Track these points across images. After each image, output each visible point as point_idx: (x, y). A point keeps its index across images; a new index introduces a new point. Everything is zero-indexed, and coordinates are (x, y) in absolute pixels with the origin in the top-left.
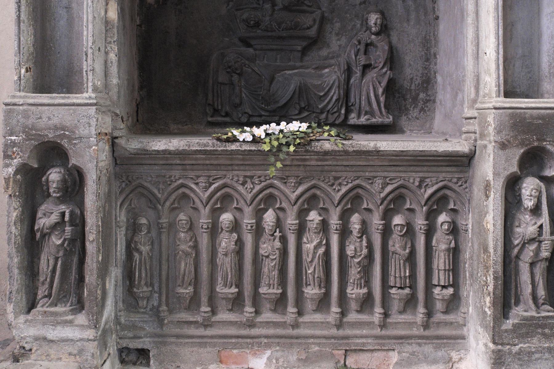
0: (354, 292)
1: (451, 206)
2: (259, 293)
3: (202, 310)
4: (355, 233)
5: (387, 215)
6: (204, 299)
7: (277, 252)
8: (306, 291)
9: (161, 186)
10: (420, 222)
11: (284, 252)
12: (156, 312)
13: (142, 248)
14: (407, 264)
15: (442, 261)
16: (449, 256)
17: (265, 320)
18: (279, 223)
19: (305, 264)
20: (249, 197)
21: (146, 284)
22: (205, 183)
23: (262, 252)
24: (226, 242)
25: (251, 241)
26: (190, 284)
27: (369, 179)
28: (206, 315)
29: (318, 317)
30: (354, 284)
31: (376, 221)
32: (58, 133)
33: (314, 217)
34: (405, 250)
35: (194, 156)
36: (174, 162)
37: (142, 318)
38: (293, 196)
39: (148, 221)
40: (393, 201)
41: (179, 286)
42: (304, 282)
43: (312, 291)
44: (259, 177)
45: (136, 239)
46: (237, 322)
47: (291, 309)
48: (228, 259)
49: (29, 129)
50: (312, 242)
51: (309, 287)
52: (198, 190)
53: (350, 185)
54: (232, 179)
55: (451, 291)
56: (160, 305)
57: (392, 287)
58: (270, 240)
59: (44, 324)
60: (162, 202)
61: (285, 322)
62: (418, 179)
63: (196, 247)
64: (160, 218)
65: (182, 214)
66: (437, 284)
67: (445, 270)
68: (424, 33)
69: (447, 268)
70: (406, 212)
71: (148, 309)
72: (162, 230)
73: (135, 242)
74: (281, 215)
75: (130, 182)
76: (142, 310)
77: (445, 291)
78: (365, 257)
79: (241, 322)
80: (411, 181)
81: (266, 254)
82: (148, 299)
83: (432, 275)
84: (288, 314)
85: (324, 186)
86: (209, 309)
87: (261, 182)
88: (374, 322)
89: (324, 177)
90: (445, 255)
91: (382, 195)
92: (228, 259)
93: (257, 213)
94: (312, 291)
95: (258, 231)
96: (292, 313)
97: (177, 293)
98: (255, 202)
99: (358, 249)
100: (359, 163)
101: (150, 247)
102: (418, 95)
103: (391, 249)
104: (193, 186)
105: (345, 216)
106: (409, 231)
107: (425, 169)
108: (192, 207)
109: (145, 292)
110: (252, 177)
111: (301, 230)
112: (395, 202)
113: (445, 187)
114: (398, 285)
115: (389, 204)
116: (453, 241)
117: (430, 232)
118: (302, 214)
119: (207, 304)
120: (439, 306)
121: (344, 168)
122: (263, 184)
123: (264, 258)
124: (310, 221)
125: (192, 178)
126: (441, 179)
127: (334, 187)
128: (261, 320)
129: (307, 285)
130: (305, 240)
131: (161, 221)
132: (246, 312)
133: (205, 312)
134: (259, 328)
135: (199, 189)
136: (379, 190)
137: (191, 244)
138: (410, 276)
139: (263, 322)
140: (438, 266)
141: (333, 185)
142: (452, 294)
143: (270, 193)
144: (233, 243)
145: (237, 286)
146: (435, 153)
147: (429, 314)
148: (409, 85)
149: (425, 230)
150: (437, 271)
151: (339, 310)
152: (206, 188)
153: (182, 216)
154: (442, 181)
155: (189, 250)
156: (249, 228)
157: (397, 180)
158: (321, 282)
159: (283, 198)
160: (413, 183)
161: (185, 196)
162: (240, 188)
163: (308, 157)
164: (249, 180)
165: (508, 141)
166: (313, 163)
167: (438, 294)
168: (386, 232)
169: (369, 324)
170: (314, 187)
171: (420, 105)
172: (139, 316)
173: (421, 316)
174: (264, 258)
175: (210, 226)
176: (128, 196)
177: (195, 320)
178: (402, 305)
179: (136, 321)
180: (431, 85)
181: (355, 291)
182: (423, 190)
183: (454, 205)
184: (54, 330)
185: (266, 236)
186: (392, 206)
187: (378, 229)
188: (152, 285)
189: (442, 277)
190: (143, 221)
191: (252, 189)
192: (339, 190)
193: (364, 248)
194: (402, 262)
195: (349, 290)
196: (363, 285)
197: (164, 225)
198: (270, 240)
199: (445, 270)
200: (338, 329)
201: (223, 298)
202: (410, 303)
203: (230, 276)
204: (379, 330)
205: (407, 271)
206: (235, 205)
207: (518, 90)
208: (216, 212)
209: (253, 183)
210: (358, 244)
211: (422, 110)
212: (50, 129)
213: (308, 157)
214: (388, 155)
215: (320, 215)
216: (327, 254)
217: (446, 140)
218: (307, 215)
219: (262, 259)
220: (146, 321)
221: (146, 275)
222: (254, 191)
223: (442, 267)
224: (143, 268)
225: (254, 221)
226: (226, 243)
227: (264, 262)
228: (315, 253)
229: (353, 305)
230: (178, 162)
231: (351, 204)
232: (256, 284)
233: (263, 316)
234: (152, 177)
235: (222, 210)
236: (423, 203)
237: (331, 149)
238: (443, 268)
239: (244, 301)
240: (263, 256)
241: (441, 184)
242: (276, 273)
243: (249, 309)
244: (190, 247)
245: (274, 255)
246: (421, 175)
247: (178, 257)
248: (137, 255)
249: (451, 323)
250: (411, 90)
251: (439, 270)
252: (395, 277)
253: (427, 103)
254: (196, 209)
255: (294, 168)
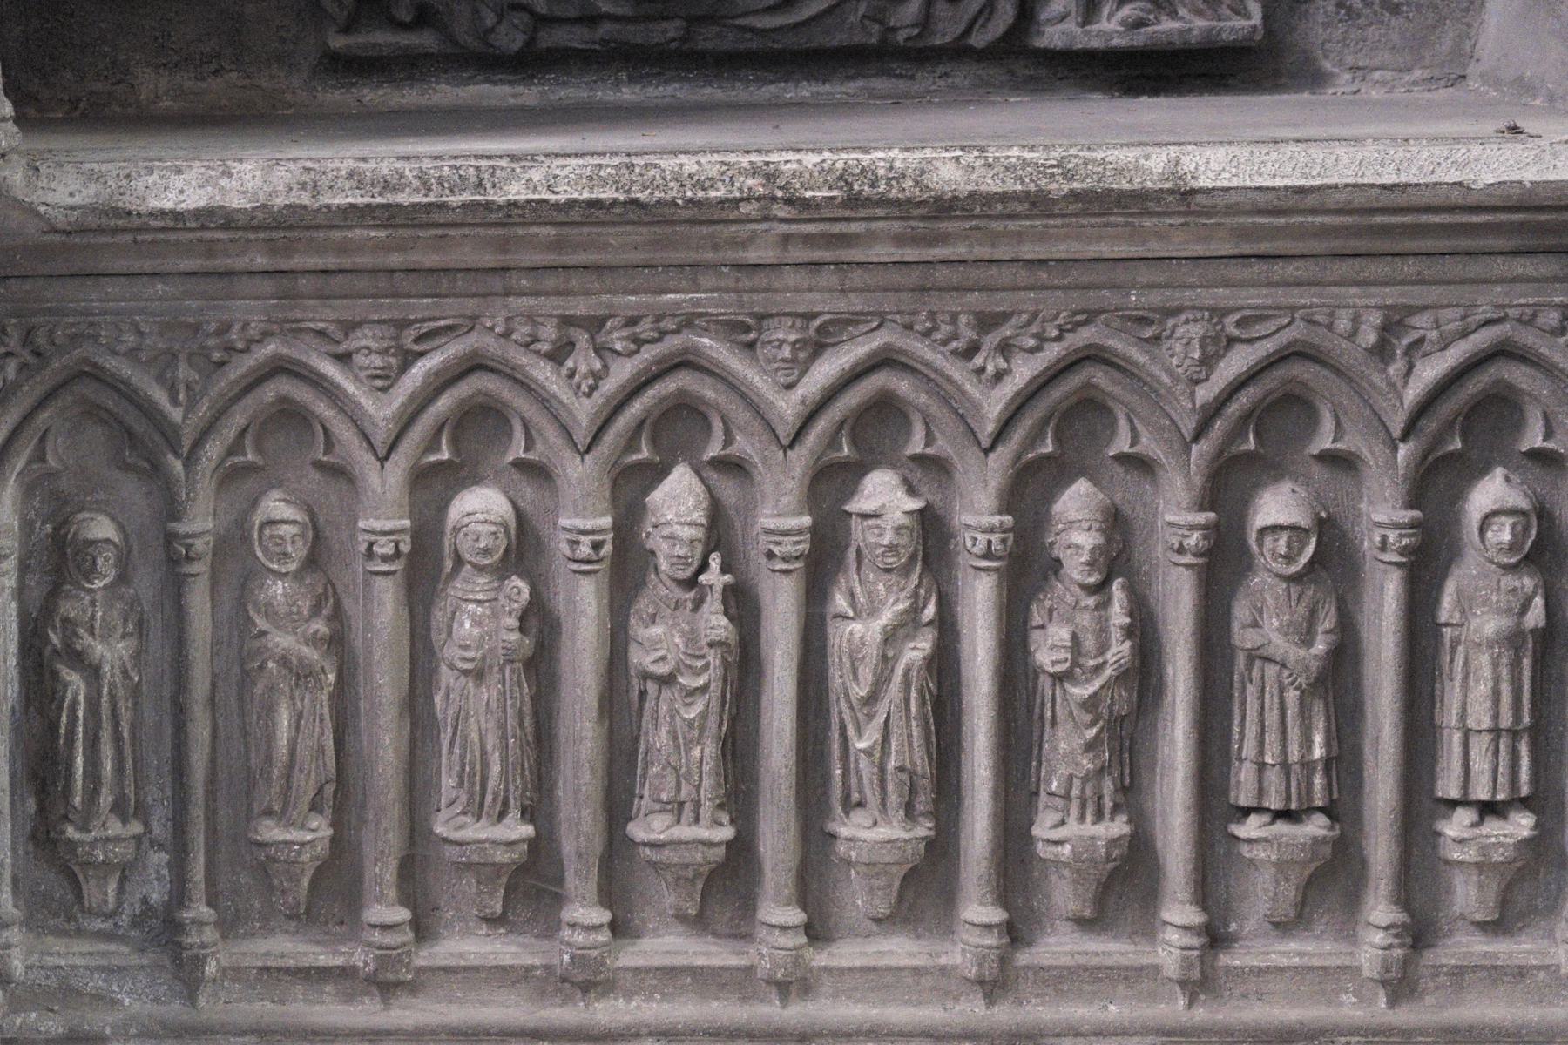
0: (1068, 833)
1: (1534, 438)
2: (633, 843)
3: (374, 919)
4: (1076, 568)
5: (1226, 488)
6: (382, 871)
7: (714, 658)
8: (844, 831)
9: (183, 372)
10: (1382, 514)
11: (745, 663)
12: (164, 930)
13: (98, 649)
14: (1318, 707)
15: (1482, 689)
16: (1515, 665)
17: (657, 961)
18: (719, 532)
19: (840, 710)
20: (584, 412)
21: (119, 808)
22: (384, 352)
23: (640, 658)
24: (477, 618)
25: (592, 610)
26: (315, 807)
27: (1143, 321)
28: (389, 939)
29: (899, 950)
30: (1067, 797)
31: (1175, 514)
33: (884, 497)
34: (1307, 642)
35: (337, 235)
36: (241, 263)
37: (104, 954)
38: (787, 407)
39: (121, 528)
40: (1259, 418)
41: (269, 813)
42: (837, 791)
43: (872, 833)
44: (632, 322)
45: (67, 608)
46: (529, 969)
47: (779, 912)
48: (489, 693)
50: (873, 612)
51: (858, 816)
52: (350, 387)
53: (1053, 352)
54: (506, 335)
55: (1522, 824)
56: (180, 894)
57: (1246, 812)
58: (678, 605)
60: (187, 443)
61: (749, 970)
62: (1376, 318)
63: (338, 643)
64: (176, 517)
65: (276, 494)
66: (1454, 793)
67: (1495, 731)
69: (1506, 721)
70: (1317, 470)
71: (124, 920)
72: (188, 569)
73: (66, 620)
74: (729, 490)
75: (37, 354)
76: (98, 924)
77: (1494, 829)
78: (1121, 677)
79: (548, 968)
80: (1343, 324)
81: (662, 669)
82: (126, 872)
83: (1434, 759)
84: (762, 932)
85: (929, 355)
86: (402, 914)
87: (639, 342)
88: (1156, 969)
89: (932, 315)
90: (1495, 665)
91: (1205, 394)
92: (489, 693)
93: (615, 484)
94: (872, 833)
95: (627, 565)
96: (784, 928)
97: (261, 845)
98: (609, 437)
99: (1089, 643)
100: (1092, 250)
101: (132, 643)
103: (1243, 638)
104: (330, 369)
105: (1028, 494)
106: (1331, 558)
107: (1410, 268)
108: (318, 465)
109: (117, 839)
110: (595, 324)
111: (823, 560)
112: (1266, 425)
113: (1501, 352)
114: (1274, 802)
115: (1237, 432)
116: (1538, 601)
117: (1427, 562)
118: (831, 484)
119: (392, 893)
120: (1468, 895)
121: (1023, 276)
122: (648, 353)
123: (651, 687)
124: (865, 516)
125: (321, 333)
126: (1485, 311)
127: (978, 361)
128: (640, 962)
129: (849, 805)
130: (840, 602)
131: (182, 528)
132: (573, 926)
133: (385, 927)
134: (629, 996)
135: (356, 378)
136: (1188, 369)
137: (320, 626)
138: (1328, 762)
139: (647, 970)
140: (1463, 716)
141: (971, 351)
142: (1526, 842)
143: (681, 392)
144: (513, 622)
145: (528, 814)
146: (1456, 197)
147: (1418, 933)
149: (1403, 551)
150: (1457, 737)
151: (996, 915)
152: (385, 380)
153: (276, 506)
154: (1488, 322)
155: (312, 654)
156: (585, 550)
157: (1271, 326)
158: (913, 791)
159: (740, 415)
160: (1352, 335)
161: (291, 416)
162: (543, 373)
163: (854, 227)
164: (582, 338)
166: (882, 252)
167: (1462, 841)
168: (1223, 563)
169: (1136, 977)
170: (884, 360)
172: (86, 946)
173: (1379, 938)
174: (651, 687)
175: (405, 548)
176: (27, 418)
177: (339, 961)
178: (1290, 892)
179: (74, 967)
181: (1073, 828)
182: (1396, 368)
183: (1548, 435)
185: (660, 589)
186: (1251, 444)
187: (1181, 550)
188: (142, 812)
189: (1481, 764)
190: (102, 528)
191: (597, 377)
192: (999, 376)
193: (1116, 634)
194: (1292, 695)
195: (1043, 828)
196: (1108, 804)
197: (199, 545)
198: (678, 605)
199: (1495, 731)
200: (990, 1000)
201: (469, 866)
202: (1330, 882)
203: (495, 769)
204: (1182, 1002)
205: (1318, 739)
206: (517, 450)
208: (433, 485)
209: (599, 351)
210: (1085, 620)
213: (854, 227)
214: (1233, 210)
215: (912, 491)
216: (945, 664)
217: (1514, 130)
218: (851, 491)
219: (643, 694)
220: (120, 969)
221: (119, 769)
222: (609, 386)
223: (1480, 717)
224: (106, 735)
225: (606, 521)
226: (477, 623)
227: (649, 705)
228: (886, 661)
229: (1065, 896)
230: (261, 262)
231: (1058, 439)
232: (617, 807)
233: (646, 943)
234: (141, 334)
235: (459, 475)
236: (1397, 428)
237: (964, 189)
238: (1486, 723)
239: (560, 880)
240: (646, 676)
241: (1482, 339)
242: (706, 751)
243: (585, 912)
244: (314, 641)
245: (697, 673)
246: (1391, 295)
247: (258, 690)
248: (74, 681)
249: (1521, 972)
251: (1467, 734)
252: (1261, 766)
254: (339, 473)
255: (791, 278)
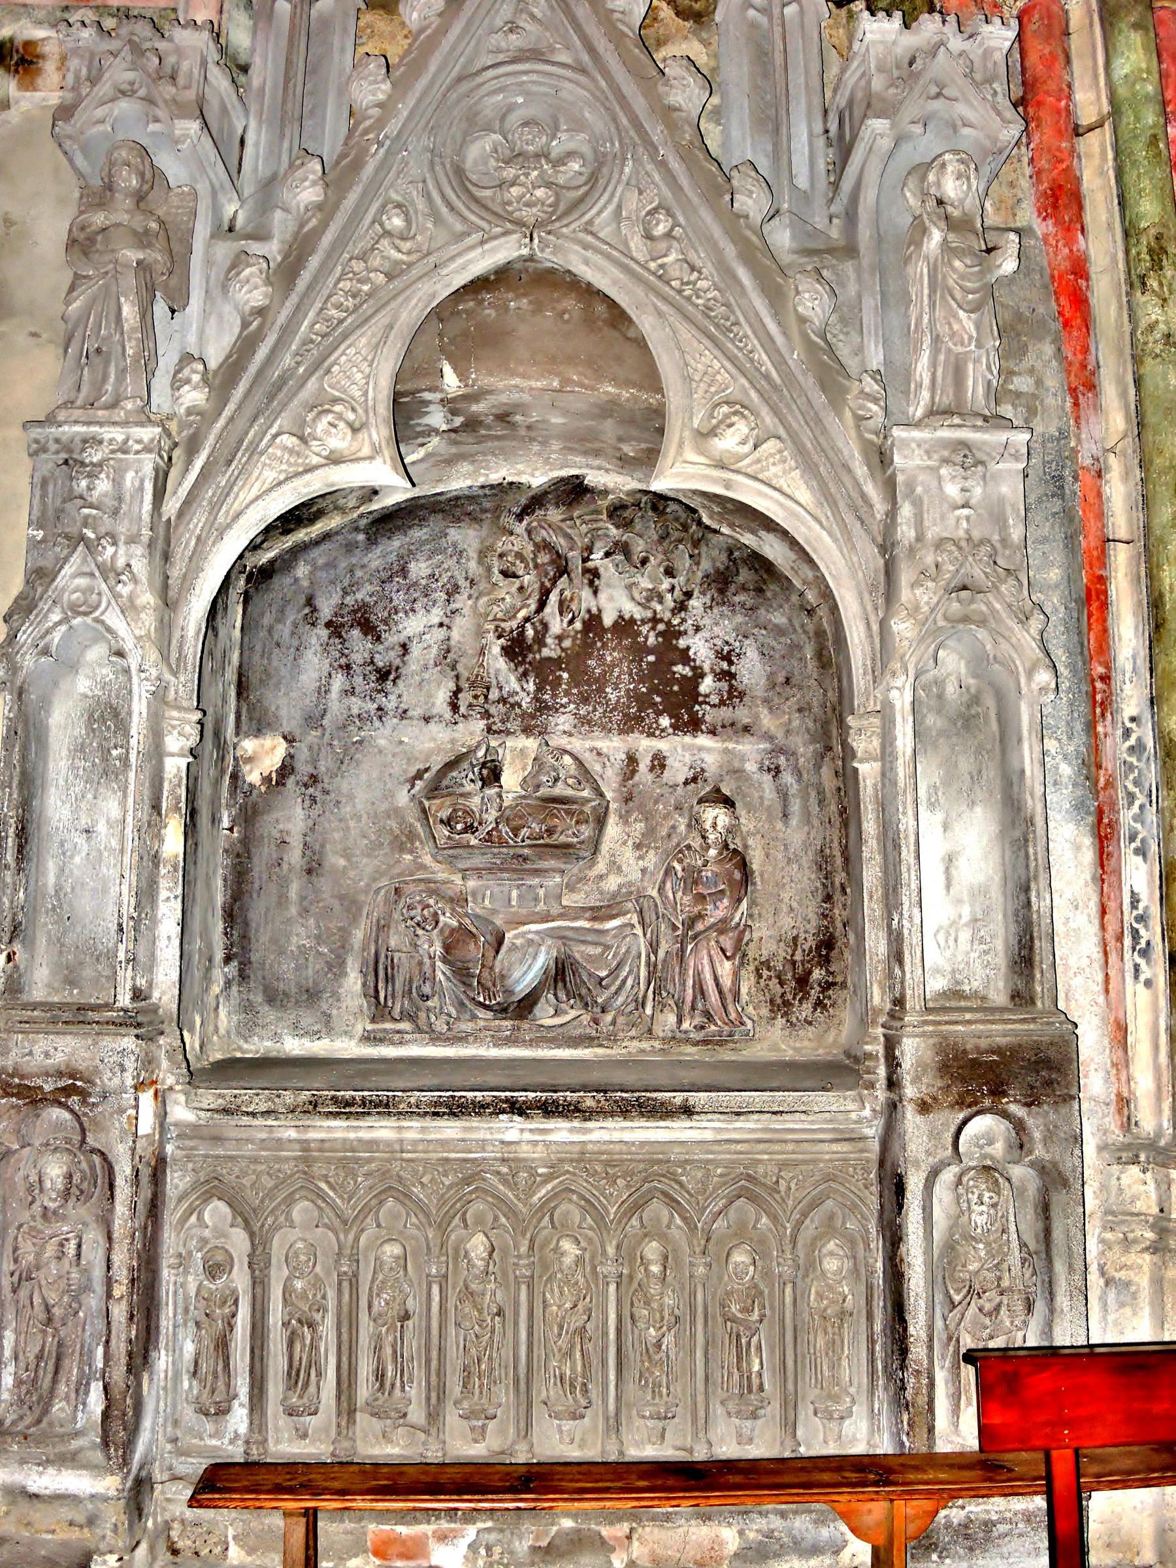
32: (61, 1084)
49: (8, 1075)
59: (23, 1462)
68: (819, 843)
102: (810, 972)
148: (790, 951)
165: (935, 1099)
171: (814, 993)
180: (836, 951)
184: (41, 1474)
207: (967, 988)
211: (819, 1004)
212: (47, 1074)
250: (794, 963)
253: (828, 988)
